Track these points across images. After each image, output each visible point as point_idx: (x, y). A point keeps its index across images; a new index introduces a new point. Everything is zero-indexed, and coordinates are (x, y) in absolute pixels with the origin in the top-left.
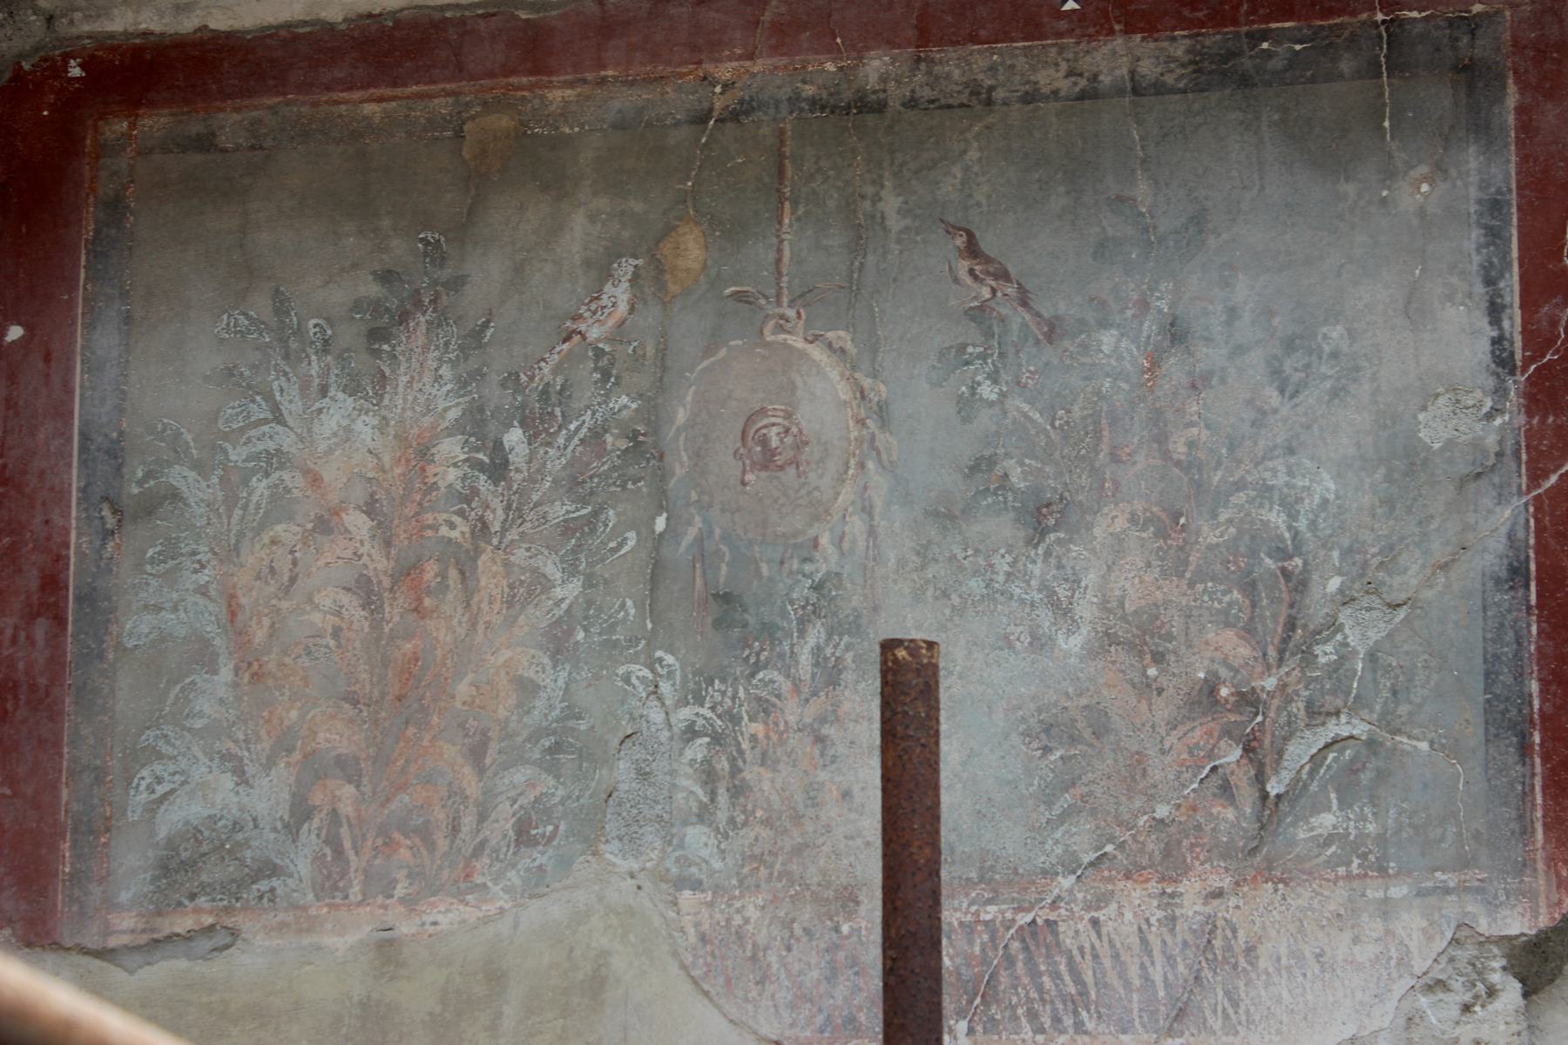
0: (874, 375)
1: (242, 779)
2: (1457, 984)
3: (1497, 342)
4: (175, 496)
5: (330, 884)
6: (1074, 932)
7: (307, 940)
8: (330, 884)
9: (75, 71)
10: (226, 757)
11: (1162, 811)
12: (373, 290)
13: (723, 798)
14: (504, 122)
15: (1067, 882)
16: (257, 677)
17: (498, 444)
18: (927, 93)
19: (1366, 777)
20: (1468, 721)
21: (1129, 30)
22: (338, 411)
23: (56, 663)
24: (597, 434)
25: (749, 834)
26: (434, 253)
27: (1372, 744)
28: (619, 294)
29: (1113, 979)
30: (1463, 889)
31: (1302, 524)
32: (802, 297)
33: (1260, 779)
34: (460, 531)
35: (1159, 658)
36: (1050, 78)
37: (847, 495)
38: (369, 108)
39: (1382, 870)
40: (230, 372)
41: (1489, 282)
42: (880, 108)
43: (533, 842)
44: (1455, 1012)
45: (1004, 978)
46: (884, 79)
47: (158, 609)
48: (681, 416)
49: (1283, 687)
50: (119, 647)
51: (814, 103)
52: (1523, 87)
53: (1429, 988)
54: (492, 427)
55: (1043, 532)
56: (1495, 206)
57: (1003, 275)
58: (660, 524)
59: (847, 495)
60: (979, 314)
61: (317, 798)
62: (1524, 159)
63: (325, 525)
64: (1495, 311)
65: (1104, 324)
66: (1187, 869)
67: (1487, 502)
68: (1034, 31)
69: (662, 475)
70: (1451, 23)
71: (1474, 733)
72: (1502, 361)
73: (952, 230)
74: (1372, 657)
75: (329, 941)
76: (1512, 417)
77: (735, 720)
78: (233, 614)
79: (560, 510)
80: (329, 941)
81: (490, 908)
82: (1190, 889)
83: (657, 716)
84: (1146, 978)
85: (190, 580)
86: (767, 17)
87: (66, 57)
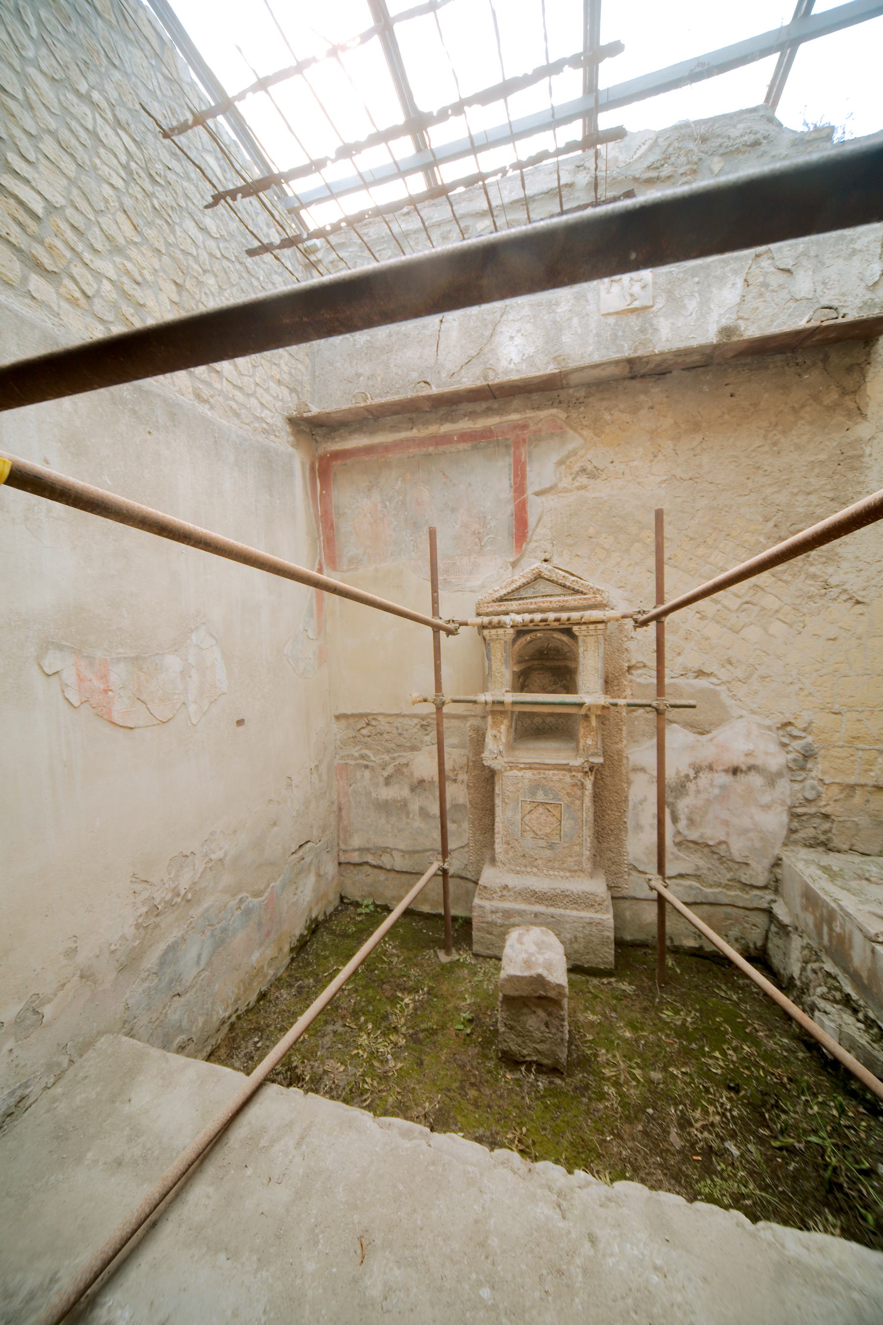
14: (383, 460)
28: (399, 483)
36: (453, 450)
56: (510, 465)
68: (451, 443)
72: (511, 486)
76: (512, 494)
79: (394, 512)
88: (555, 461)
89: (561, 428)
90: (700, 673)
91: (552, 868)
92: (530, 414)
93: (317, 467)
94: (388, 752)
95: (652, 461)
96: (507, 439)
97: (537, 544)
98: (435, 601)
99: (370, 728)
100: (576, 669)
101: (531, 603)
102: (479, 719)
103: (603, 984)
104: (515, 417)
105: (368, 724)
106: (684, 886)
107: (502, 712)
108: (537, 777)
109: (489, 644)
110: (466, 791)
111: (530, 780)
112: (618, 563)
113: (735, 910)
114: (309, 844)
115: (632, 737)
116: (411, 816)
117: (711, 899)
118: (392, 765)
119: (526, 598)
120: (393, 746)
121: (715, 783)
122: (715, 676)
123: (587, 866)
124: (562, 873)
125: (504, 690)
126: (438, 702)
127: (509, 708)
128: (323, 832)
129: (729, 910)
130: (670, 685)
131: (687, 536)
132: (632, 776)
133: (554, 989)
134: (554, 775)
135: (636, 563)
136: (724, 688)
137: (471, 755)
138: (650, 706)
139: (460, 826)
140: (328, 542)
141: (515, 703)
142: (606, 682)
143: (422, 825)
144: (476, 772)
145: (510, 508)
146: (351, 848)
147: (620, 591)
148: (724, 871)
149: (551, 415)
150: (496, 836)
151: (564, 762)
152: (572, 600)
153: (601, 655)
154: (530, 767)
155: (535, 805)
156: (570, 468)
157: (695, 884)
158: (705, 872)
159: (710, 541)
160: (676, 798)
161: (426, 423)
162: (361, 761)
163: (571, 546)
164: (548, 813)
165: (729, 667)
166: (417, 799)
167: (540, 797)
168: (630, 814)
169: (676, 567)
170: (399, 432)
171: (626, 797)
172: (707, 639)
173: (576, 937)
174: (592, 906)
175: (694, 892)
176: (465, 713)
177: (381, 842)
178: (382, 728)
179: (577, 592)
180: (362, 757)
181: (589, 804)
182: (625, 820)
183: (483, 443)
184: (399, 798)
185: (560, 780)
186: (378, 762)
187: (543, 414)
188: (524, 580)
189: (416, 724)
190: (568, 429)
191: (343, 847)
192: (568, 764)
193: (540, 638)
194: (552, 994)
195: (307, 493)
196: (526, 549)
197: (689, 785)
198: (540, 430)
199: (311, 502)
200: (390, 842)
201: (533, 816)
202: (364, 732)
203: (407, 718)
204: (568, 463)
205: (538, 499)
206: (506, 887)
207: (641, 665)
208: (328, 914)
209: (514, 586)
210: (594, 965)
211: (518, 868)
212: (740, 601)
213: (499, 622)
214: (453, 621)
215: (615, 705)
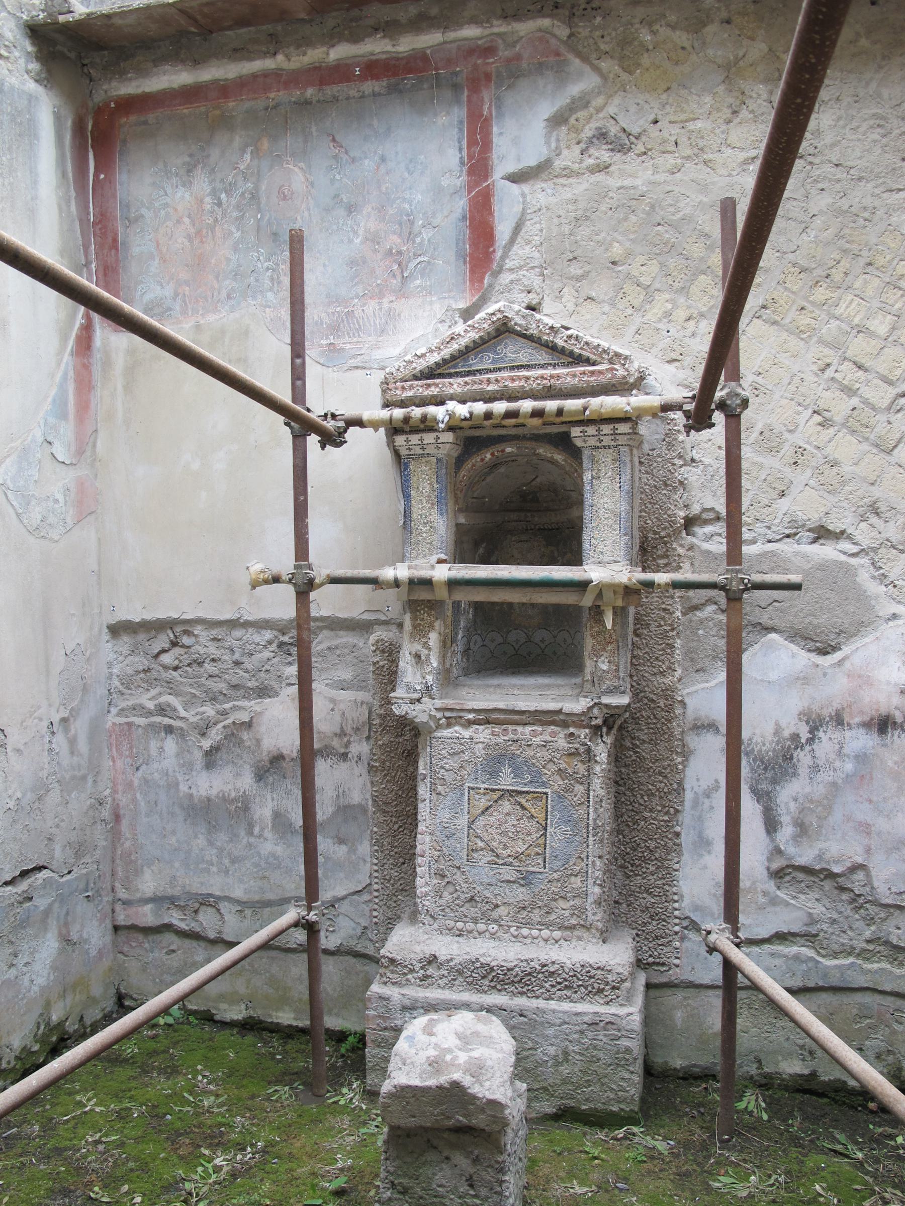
0: (310, 174)
1: (163, 287)
2: (448, 321)
3: (461, 158)
4: (143, 216)
5: (184, 312)
6: (358, 313)
7: (180, 326)
8: (184, 312)
9: (113, 105)
10: (158, 282)
11: (379, 282)
12: (187, 159)
13: (275, 285)
14: (218, 112)
15: (356, 301)
16: (164, 261)
17: (219, 198)
18: (322, 98)
19: (427, 271)
20: (451, 255)
21: (372, 79)
22: (181, 192)
23: (117, 261)
24: (243, 194)
25: (282, 293)
26: (202, 149)
27: (429, 262)
28: (247, 157)
29: (367, 324)
30: (449, 297)
31: (413, 207)
32: (292, 155)
33: (402, 272)
34: (211, 221)
35: (378, 243)
36: (353, 93)
37: (304, 206)
38: (185, 111)
39: (430, 294)
40: (154, 183)
41: (459, 142)
42: (311, 103)
43: (231, 298)
44: (447, 328)
45: (342, 325)
46: (312, 95)
47: (140, 245)
48: (263, 188)
49: (408, 249)
50: (131, 256)
51: (295, 103)
52: (469, 90)
53: (441, 322)
54: (218, 193)
55: (351, 212)
56: (461, 122)
57: (341, 146)
58: (259, 216)
59: (304, 206)
60: (335, 157)
61: (180, 291)
62: (469, 110)
63: (179, 221)
64: (460, 150)
65: (366, 158)
66: (384, 296)
67: (457, 199)
69: (259, 204)
70: (451, 74)
71: (453, 258)
72: (462, 163)
73: (329, 135)
74: (429, 240)
75: (184, 326)
76: (464, 178)
77: (278, 265)
78: (158, 246)
79: (235, 214)
80: (184, 326)
81: (222, 316)
82: (385, 300)
83: (260, 265)
84: (375, 323)
85: (147, 238)
86: (282, 80)
87: (111, 101)
88: (546, 117)
89: (558, 54)
90: (822, 534)
91: (528, 924)
92: (500, 27)
93: (90, 128)
94: (214, 699)
95: (729, 122)
96: (456, 74)
97: (513, 276)
98: (298, 375)
99: (177, 651)
100: (581, 518)
101: (489, 381)
102: (394, 628)
103: (615, 1139)
104: (470, 32)
105: (174, 644)
106: (785, 956)
107: (434, 606)
108: (500, 740)
109: (406, 466)
110: (366, 777)
111: (487, 747)
112: (668, 314)
113: (878, 998)
114: (45, 874)
115: (692, 660)
116: (256, 830)
117: (835, 981)
118: (221, 724)
119: (480, 372)
120: (222, 686)
121: (846, 750)
122: (849, 538)
123: (596, 916)
124: (546, 933)
125: (434, 558)
126: (300, 579)
127: (442, 594)
128: (78, 855)
129: (868, 999)
130: (763, 555)
131: (794, 265)
132: (693, 741)
133: (483, 1110)
134: (534, 734)
135: (702, 315)
136: (864, 561)
137: (376, 703)
138: (713, 586)
139: (353, 850)
140: (105, 275)
141: (453, 584)
142: (643, 550)
143: (279, 850)
144: (386, 739)
145: (461, 204)
146: (138, 895)
147: (671, 368)
148: (860, 924)
149: (540, 30)
150: (419, 860)
151: (552, 706)
152: (567, 375)
153: (626, 487)
154: (487, 718)
155: (495, 796)
156: (577, 131)
157: (811, 953)
158: (825, 926)
159: (837, 275)
160: (775, 781)
161: (305, 43)
162: (158, 719)
163: (579, 279)
164: (520, 812)
165: (874, 520)
166: (269, 797)
167: (506, 781)
168: (687, 817)
169: (775, 323)
170: (250, 59)
171: (680, 783)
172: (834, 464)
173: (566, 1053)
174: (600, 991)
175: (804, 967)
176: (366, 616)
177: (198, 884)
178: (202, 650)
179: (579, 360)
180: (162, 710)
181: (602, 792)
182: (678, 829)
183: (410, 80)
184: (233, 794)
185: (545, 745)
186: (192, 720)
187: (525, 28)
188: (474, 335)
189: (270, 642)
190: (571, 57)
191: (122, 894)
192: (560, 712)
193: (511, 460)
194: (479, 1121)
195: (64, 174)
196: (491, 286)
197: (799, 755)
198: (518, 57)
199: (73, 194)
200: (215, 885)
201: (492, 819)
202: (166, 659)
203: (250, 630)
204: (572, 121)
205: (515, 189)
206: (432, 960)
207: (712, 515)
208: (88, 1021)
209: (455, 346)
210: (600, 1106)
211: (460, 925)
212: (892, 392)
213: (424, 418)
214: (334, 416)
215: (650, 585)
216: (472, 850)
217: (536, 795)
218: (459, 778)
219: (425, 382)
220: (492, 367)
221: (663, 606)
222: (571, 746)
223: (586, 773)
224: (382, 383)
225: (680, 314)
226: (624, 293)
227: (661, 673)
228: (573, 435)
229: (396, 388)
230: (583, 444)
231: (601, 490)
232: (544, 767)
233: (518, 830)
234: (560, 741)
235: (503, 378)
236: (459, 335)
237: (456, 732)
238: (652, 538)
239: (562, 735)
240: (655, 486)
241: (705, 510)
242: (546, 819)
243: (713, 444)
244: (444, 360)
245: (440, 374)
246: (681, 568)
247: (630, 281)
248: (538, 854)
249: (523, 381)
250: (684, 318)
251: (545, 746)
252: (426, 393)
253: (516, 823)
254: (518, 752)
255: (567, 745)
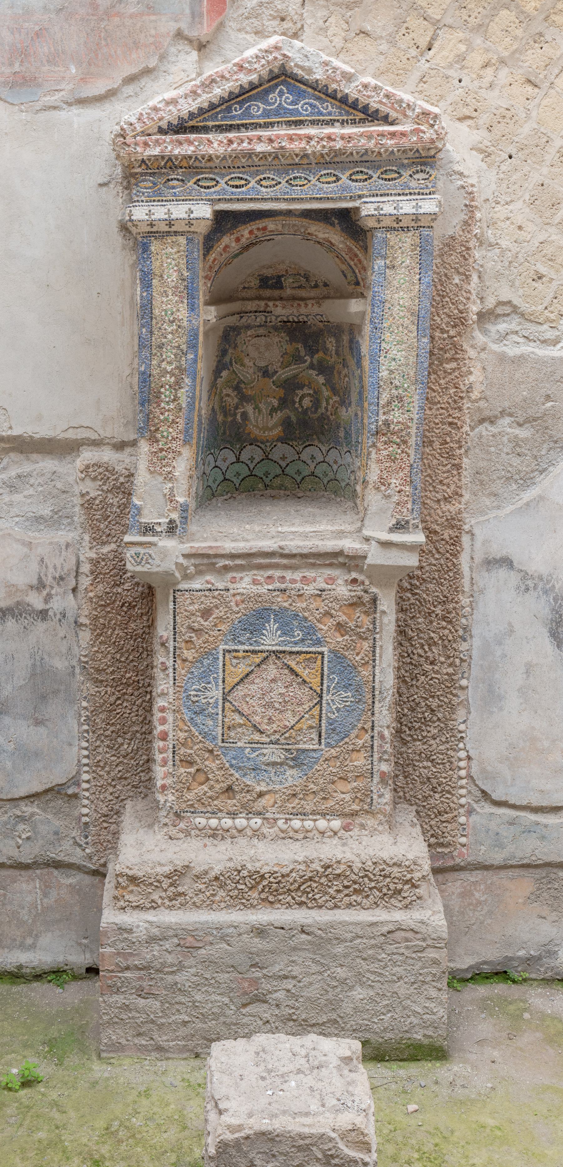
108: (263, 589)
112: (461, 58)
115: (482, 483)
119: (246, 126)
147: (463, 127)
164: (290, 677)
207: (508, 309)
209: (218, 92)
216: (229, 728)
217: (308, 656)
218: (211, 639)
219: (175, 137)
220: (261, 121)
221: (450, 420)
222: (353, 594)
223: (371, 627)
224: (117, 136)
225: (476, 59)
226: (407, 28)
227: (445, 499)
228: (364, 213)
229: (136, 144)
230: (376, 225)
231: (395, 283)
232: (319, 621)
233: (287, 699)
234: (339, 589)
235: (278, 137)
236: (223, 77)
237: (208, 582)
238: (440, 338)
239: (340, 582)
240: (446, 275)
241: (500, 303)
242: (322, 684)
243: (512, 223)
244: (200, 109)
245: (193, 127)
246: (471, 373)
247: (415, 13)
248: (311, 727)
249: (304, 142)
250: (480, 64)
251: (320, 596)
252: (176, 152)
253: (283, 691)
254: (286, 604)
255: (347, 593)
